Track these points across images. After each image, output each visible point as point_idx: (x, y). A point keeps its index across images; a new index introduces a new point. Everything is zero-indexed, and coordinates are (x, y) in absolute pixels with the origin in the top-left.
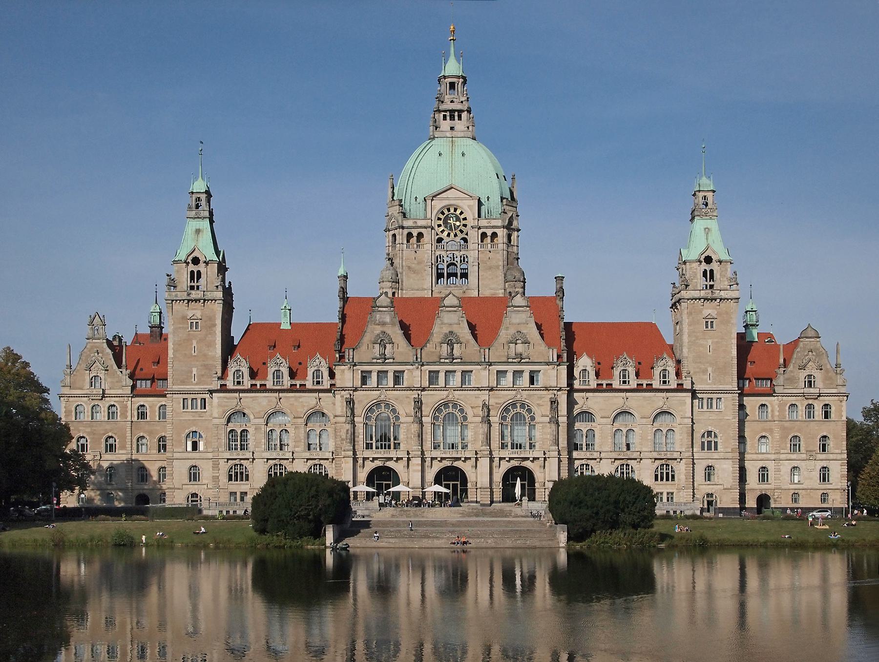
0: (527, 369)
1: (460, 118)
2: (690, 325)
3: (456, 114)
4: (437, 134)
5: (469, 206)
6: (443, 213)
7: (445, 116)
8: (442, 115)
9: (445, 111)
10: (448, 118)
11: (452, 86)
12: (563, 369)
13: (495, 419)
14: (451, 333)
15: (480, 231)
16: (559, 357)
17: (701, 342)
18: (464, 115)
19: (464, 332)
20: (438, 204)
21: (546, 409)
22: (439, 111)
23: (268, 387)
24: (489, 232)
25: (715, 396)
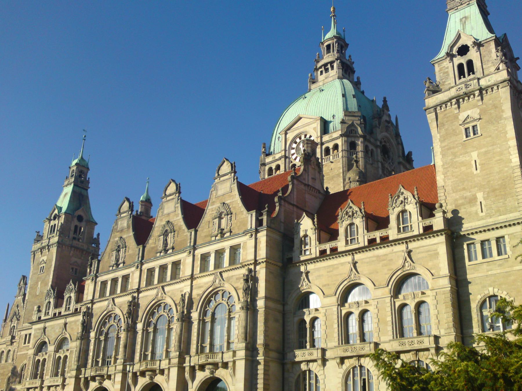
0: (226, 244)
1: (332, 68)
2: (441, 141)
3: (329, 66)
4: (313, 86)
5: (315, 129)
6: (296, 143)
7: (322, 72)
8: (319, 72)
9: (321, 67)
10: (324, 72)
11: (328, 47)
12: (262, 236)
13: (195, 315)
14: (168, 222)
15: (324, 147)
16: (259, 223)
17: (462, 159)
18: (335, 65)
19: (178, 219)
20: (291, 136)
21: (241, 293)
22: (317, 69)
23: (62, 314)
24: (331, 145)
25: (492, 235)
